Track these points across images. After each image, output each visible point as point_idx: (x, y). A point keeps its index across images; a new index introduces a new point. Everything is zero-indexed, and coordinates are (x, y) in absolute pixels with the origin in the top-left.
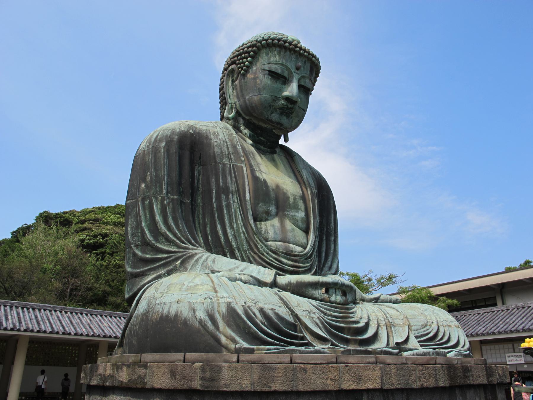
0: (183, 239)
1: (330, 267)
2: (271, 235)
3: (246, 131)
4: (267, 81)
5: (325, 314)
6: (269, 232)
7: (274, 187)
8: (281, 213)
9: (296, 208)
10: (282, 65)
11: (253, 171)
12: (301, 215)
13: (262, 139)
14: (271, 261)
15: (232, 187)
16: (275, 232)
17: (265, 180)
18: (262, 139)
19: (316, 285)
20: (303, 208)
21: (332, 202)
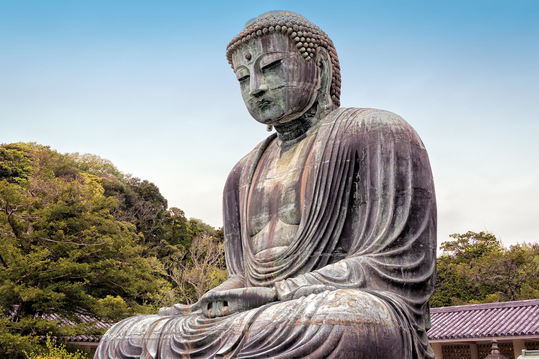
0: (232, 270)
1: (369, 244)
2: (259, 245)
3: (278, 134)
5: (185, 332)
6: (259, 243)
8: (275, 216)
9: (286, 202)
10: (239, 68)
11: (256, 185)
12: (292, 207)
13: (286, 133)
14: (253, 274)
16: (263, 242)
17: (263, 189)
18: (286, 133)
20: (293, 200)
21: (379, 151)
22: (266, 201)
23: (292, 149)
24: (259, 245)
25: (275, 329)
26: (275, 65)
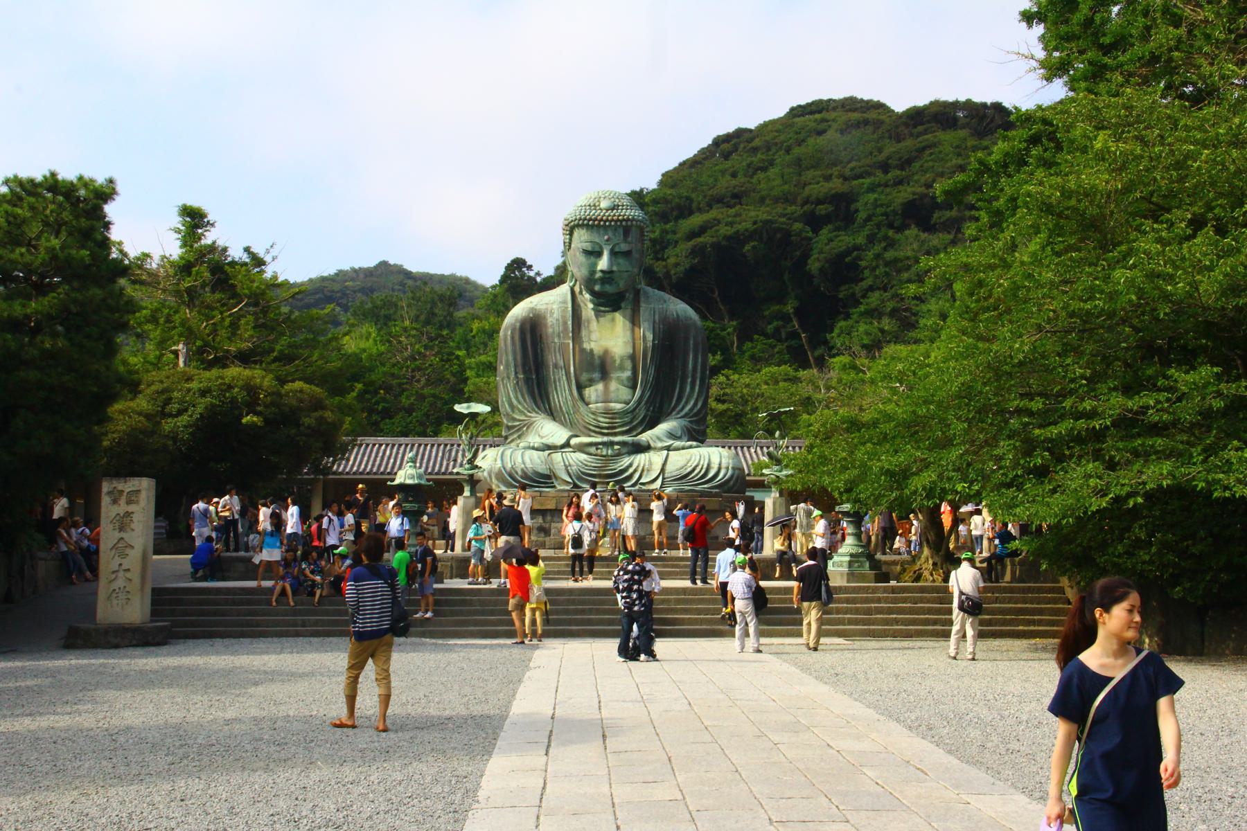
2: (593, 398)
3: (587, 296)
4: (582, 258)
7: (601, 353)
9: (622, 368)
11: (581, 343)
12: (628, 373)
15: (561, 363)
17: (592, 350)
19: (591, 444)
22: (597, 362)
23: (609, 316)
24: (593, 398)
25: (694, 470)
26: (627, 254)
